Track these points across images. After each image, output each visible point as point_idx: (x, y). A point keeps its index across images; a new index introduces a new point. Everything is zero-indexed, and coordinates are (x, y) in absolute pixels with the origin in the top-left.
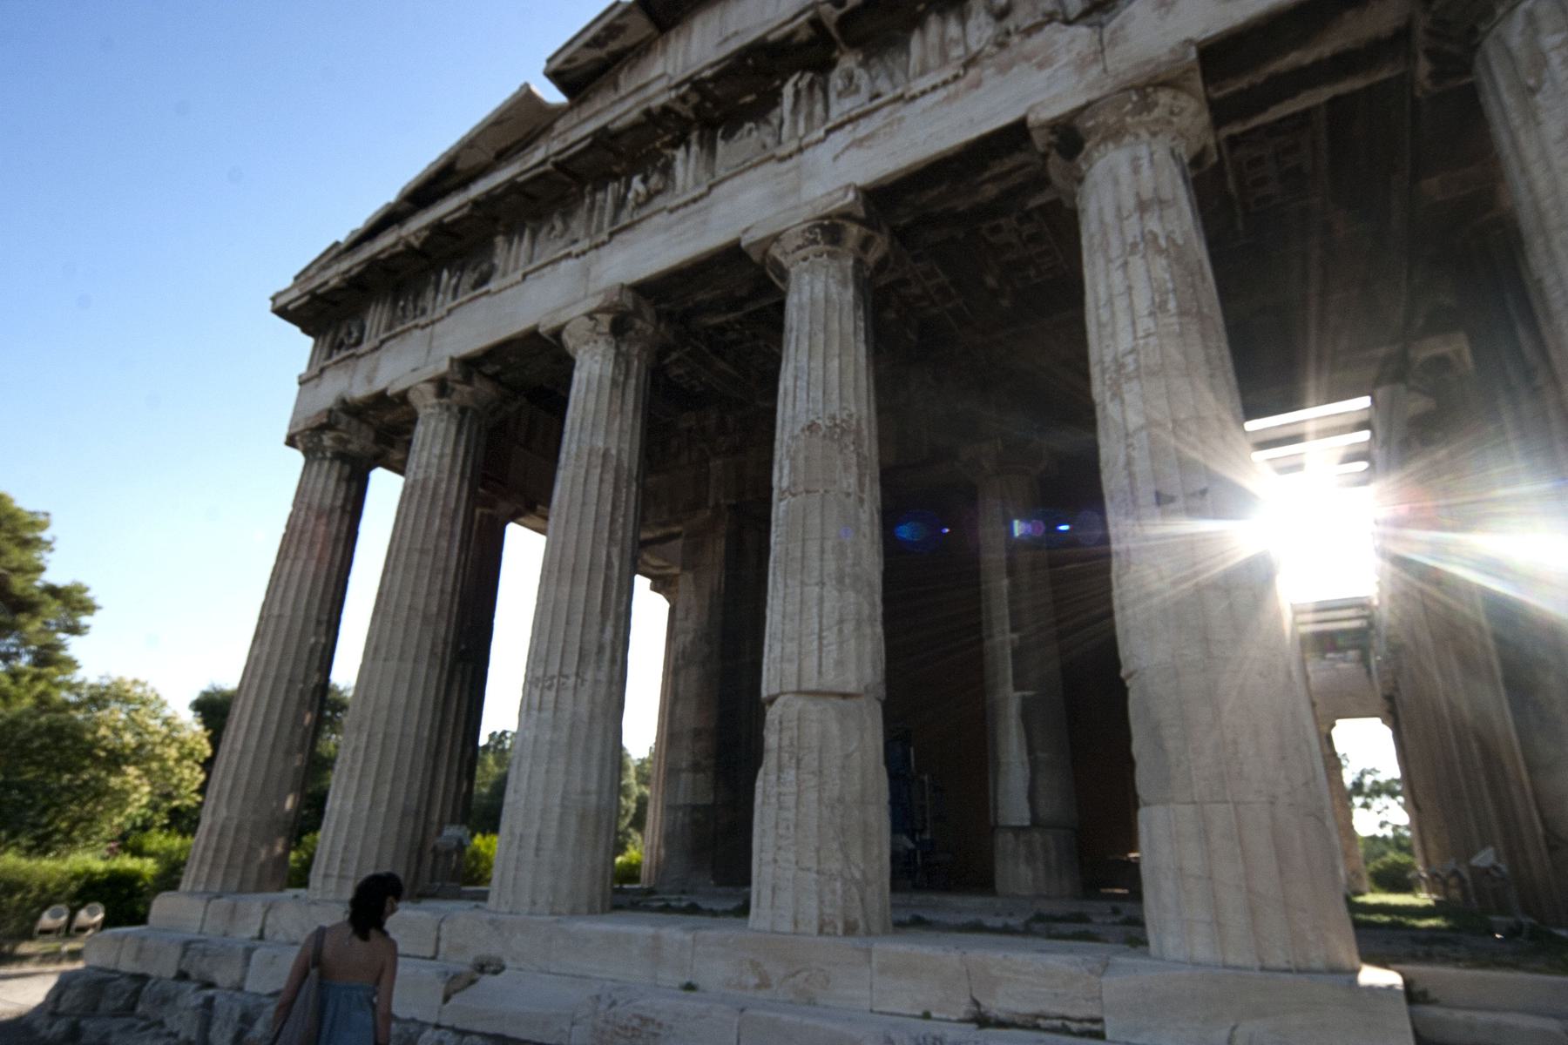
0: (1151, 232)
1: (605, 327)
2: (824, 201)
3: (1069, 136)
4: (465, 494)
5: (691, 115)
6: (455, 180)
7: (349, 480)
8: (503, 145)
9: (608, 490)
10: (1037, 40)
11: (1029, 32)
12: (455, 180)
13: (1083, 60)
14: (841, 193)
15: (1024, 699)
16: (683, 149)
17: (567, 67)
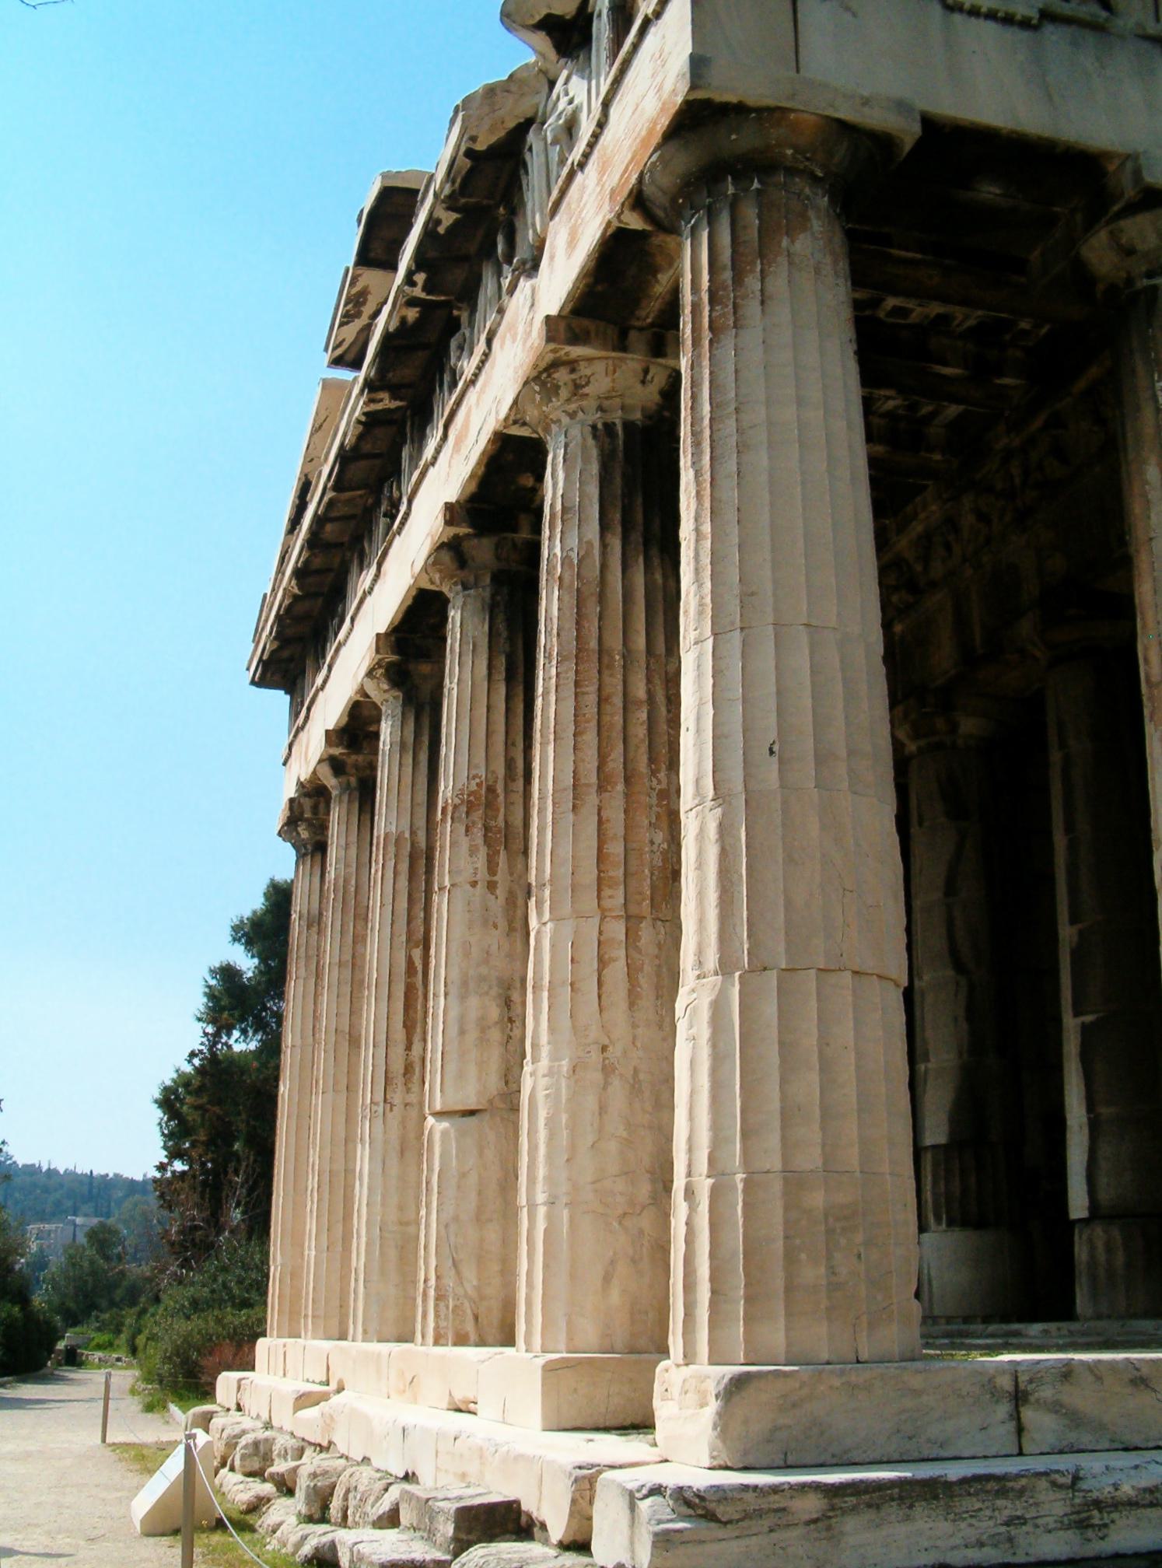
9: (403, 882)
15: (1085, 1029)
17: (339, 351)
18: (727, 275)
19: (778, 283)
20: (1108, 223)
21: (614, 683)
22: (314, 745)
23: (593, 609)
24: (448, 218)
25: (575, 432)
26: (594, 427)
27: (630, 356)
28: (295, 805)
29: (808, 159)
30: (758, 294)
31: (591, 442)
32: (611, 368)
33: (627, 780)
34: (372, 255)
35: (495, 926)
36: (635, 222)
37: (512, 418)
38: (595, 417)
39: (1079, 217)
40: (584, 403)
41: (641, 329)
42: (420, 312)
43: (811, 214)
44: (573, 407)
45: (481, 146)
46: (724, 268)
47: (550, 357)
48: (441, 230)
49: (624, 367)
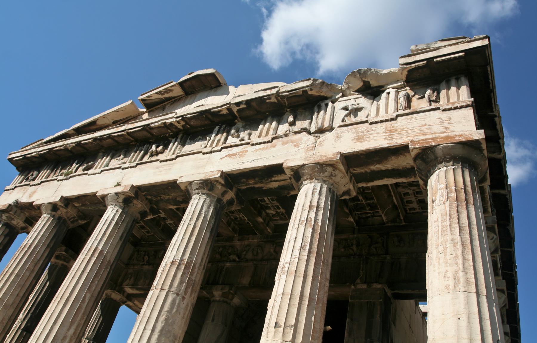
0: (310, 217)
1: (120, 200)
2: (210, 174)
3: (298, 174)
4: (46, 255)
5: (181, 128)
6: (94, 127)
7: (6, 236)
8: (117, 119)
10: (298, 136)
11: (296, 133)
12: (94, 127)
13: (308, 148)
14: (216, 172)
16: (175, 139)
17: (147, 98)
24: (273, 100)
28: (10, 207)
35: (180, 314)
40: (330, 180)
41: (350, 172)
42: (227, 114)
44: (325, 179)
48: (268, 101)
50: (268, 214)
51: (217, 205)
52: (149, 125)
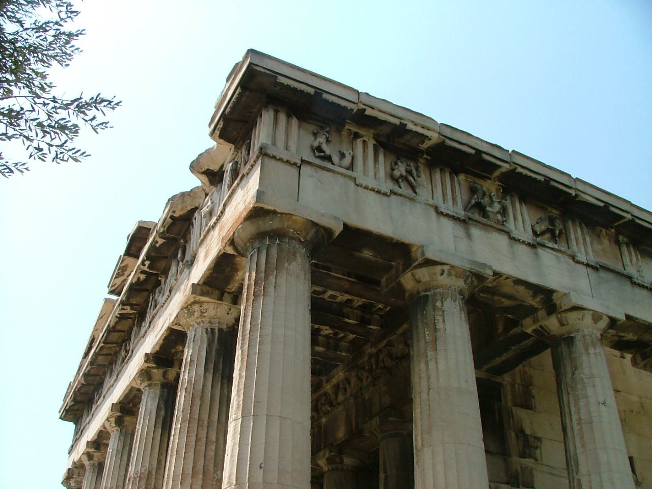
17: (113, 288)
18: (263, 275)
19: (282, 280)
20: (412, 270)
21: (203, 434)
22: (82, 446)
23: (198, 402)
24: (161, 241)
25: (199, 330)
26: (207, 329)
27: (224, 303)
29: (298, 234)
30: (274, 284)
31: (205, 335)
32: (216, 307)
33: (204, 474)
34: (131, 252)
36: (230, 251)
37: (175, 322)
38: (208, 325)
39: (401, 267)
40: (204, 319)
41: (229, 293)
42: (146, 277)
43: (298, 255)
44: (199, 321)
45: (176, 215)
46: (262, 272)
47: (193, 300)
48: (158, 245)
49: (221, 307)
50: (327, 336)
51: (163, 392)
52: (109, 326)
